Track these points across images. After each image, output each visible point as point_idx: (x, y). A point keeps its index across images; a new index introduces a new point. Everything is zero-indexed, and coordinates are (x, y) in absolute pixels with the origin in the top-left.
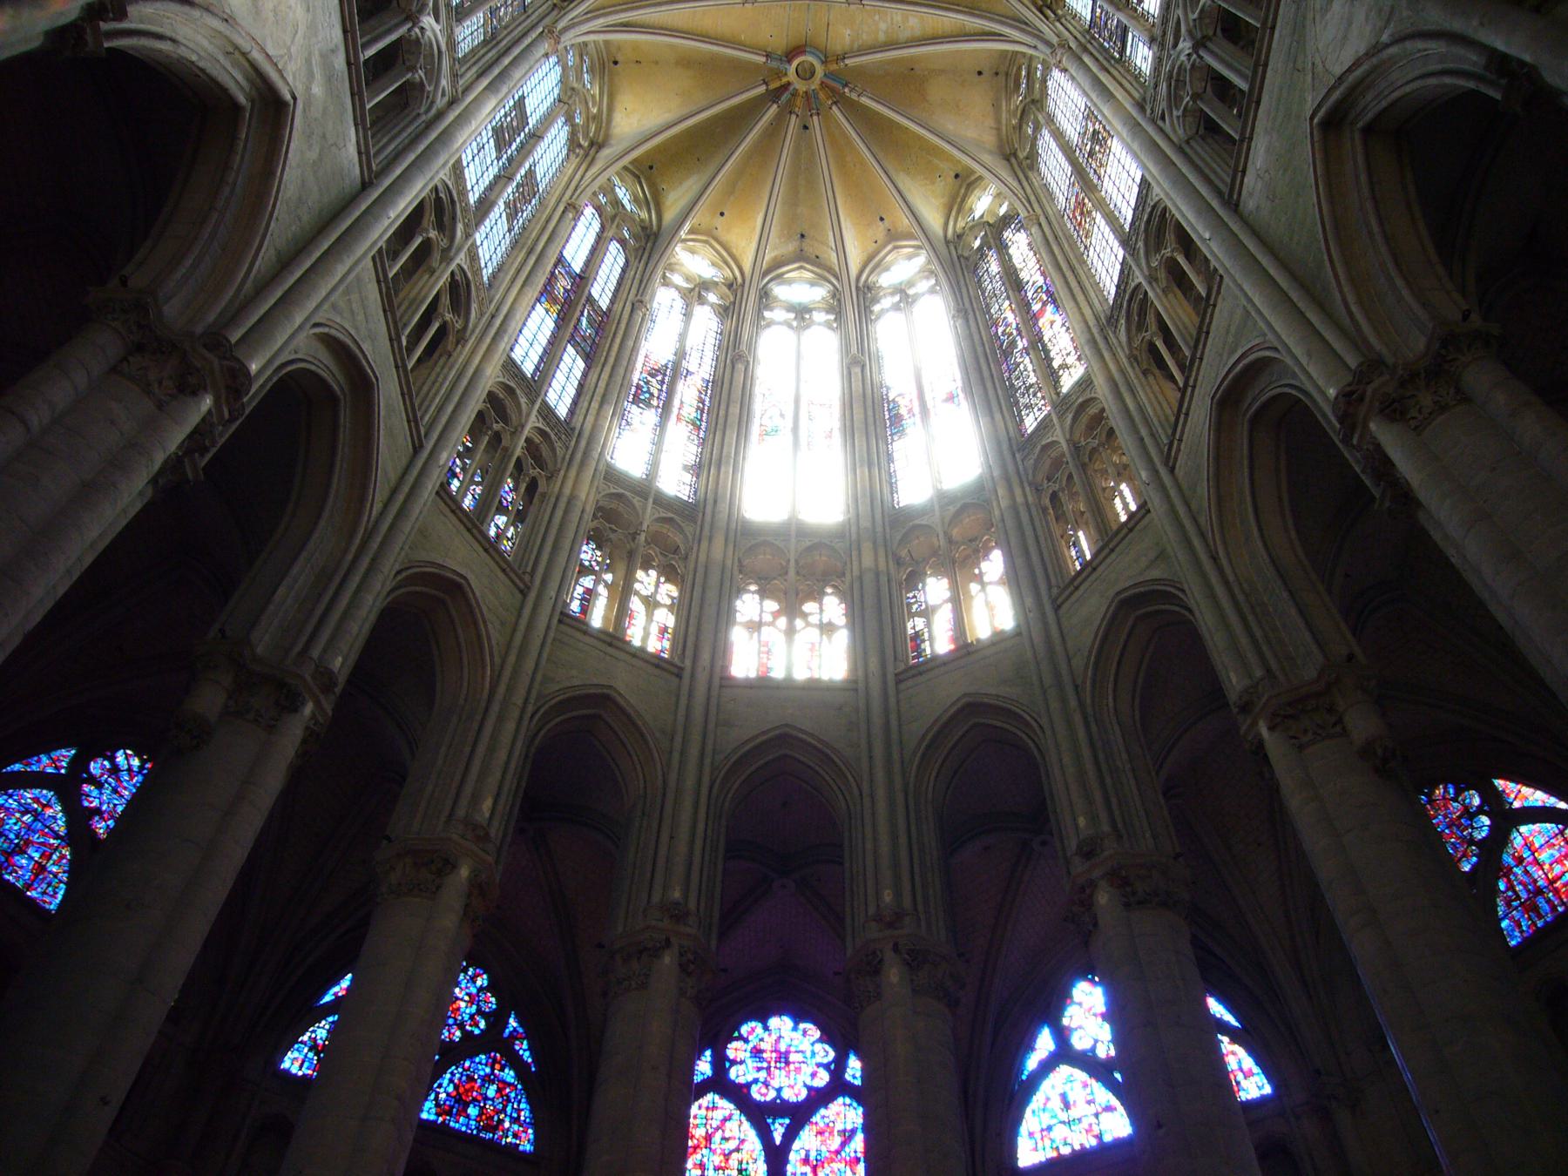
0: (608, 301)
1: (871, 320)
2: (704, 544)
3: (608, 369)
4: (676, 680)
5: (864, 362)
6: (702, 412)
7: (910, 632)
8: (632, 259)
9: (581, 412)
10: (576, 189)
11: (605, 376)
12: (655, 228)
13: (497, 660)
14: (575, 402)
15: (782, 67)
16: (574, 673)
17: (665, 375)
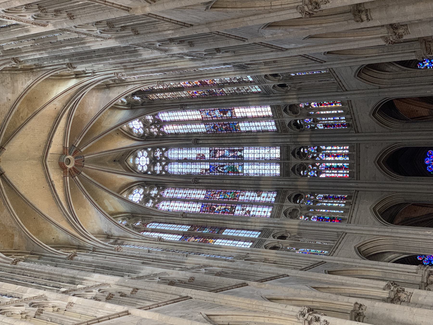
0: (183, 226)
1: (163, 136)
2: (299, 187)
3: (225, 222)
4: (359, 192)
5: (195, 139)
6: (226, 192)
7: (322, 127)
8: (151, 221)
9: (257, 228)
10: (147, 240)
11: (230, 222)
12: (130, 214)
13: (375, 237)
14: (254, 230)
15: (68, 170)
16: (369, 218)
17: (212, 205)
